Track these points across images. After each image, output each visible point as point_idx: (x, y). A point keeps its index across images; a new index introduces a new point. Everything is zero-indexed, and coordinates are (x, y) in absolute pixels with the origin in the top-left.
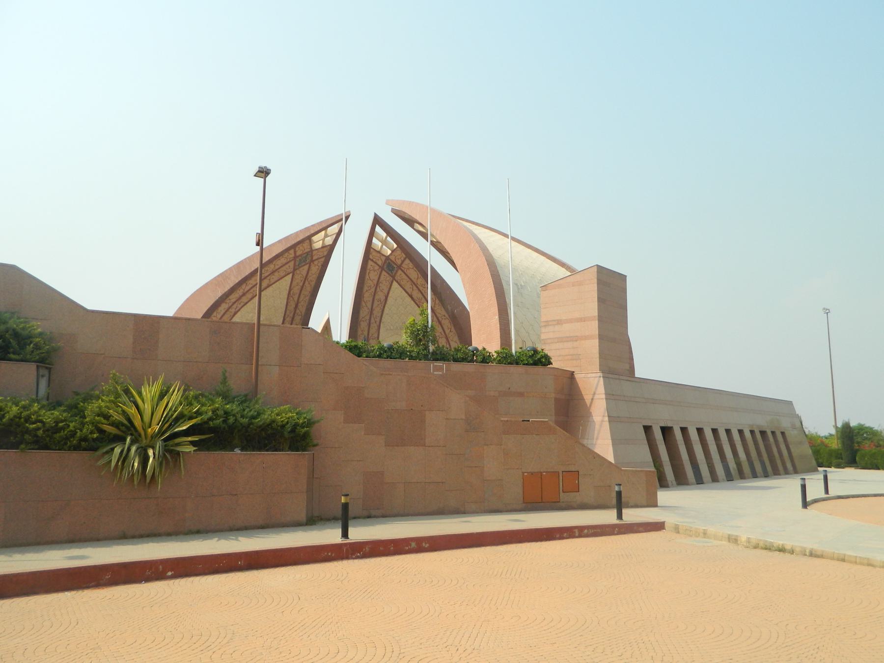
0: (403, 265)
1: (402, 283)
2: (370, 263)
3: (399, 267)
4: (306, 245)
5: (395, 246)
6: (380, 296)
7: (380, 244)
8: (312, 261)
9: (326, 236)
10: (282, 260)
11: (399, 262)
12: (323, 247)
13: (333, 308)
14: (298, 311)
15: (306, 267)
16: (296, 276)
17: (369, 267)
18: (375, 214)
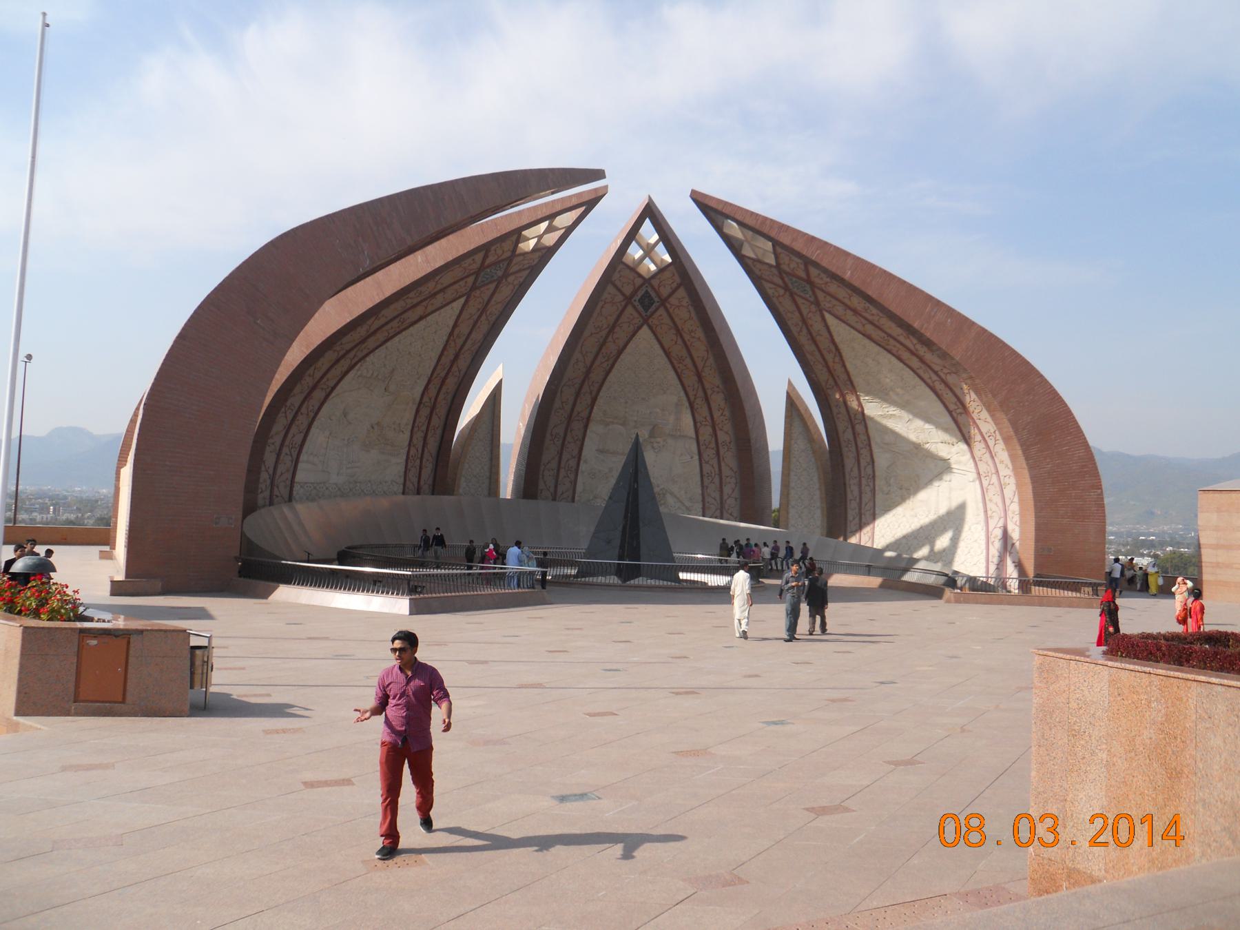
0: (673, 300)
2: (610, 289)
3: (664, 302)
4: (508, 245)
5: (667, 258)
6: (611, 347)
7: (641, 252)
8: (506, 275)
10: (457, 272)
11: (665, 292)
12: (535, 250)
13: (517, 366)
14: (455, 369)
16: (471, 303)
17: (605, 295)
18: (650, 198)
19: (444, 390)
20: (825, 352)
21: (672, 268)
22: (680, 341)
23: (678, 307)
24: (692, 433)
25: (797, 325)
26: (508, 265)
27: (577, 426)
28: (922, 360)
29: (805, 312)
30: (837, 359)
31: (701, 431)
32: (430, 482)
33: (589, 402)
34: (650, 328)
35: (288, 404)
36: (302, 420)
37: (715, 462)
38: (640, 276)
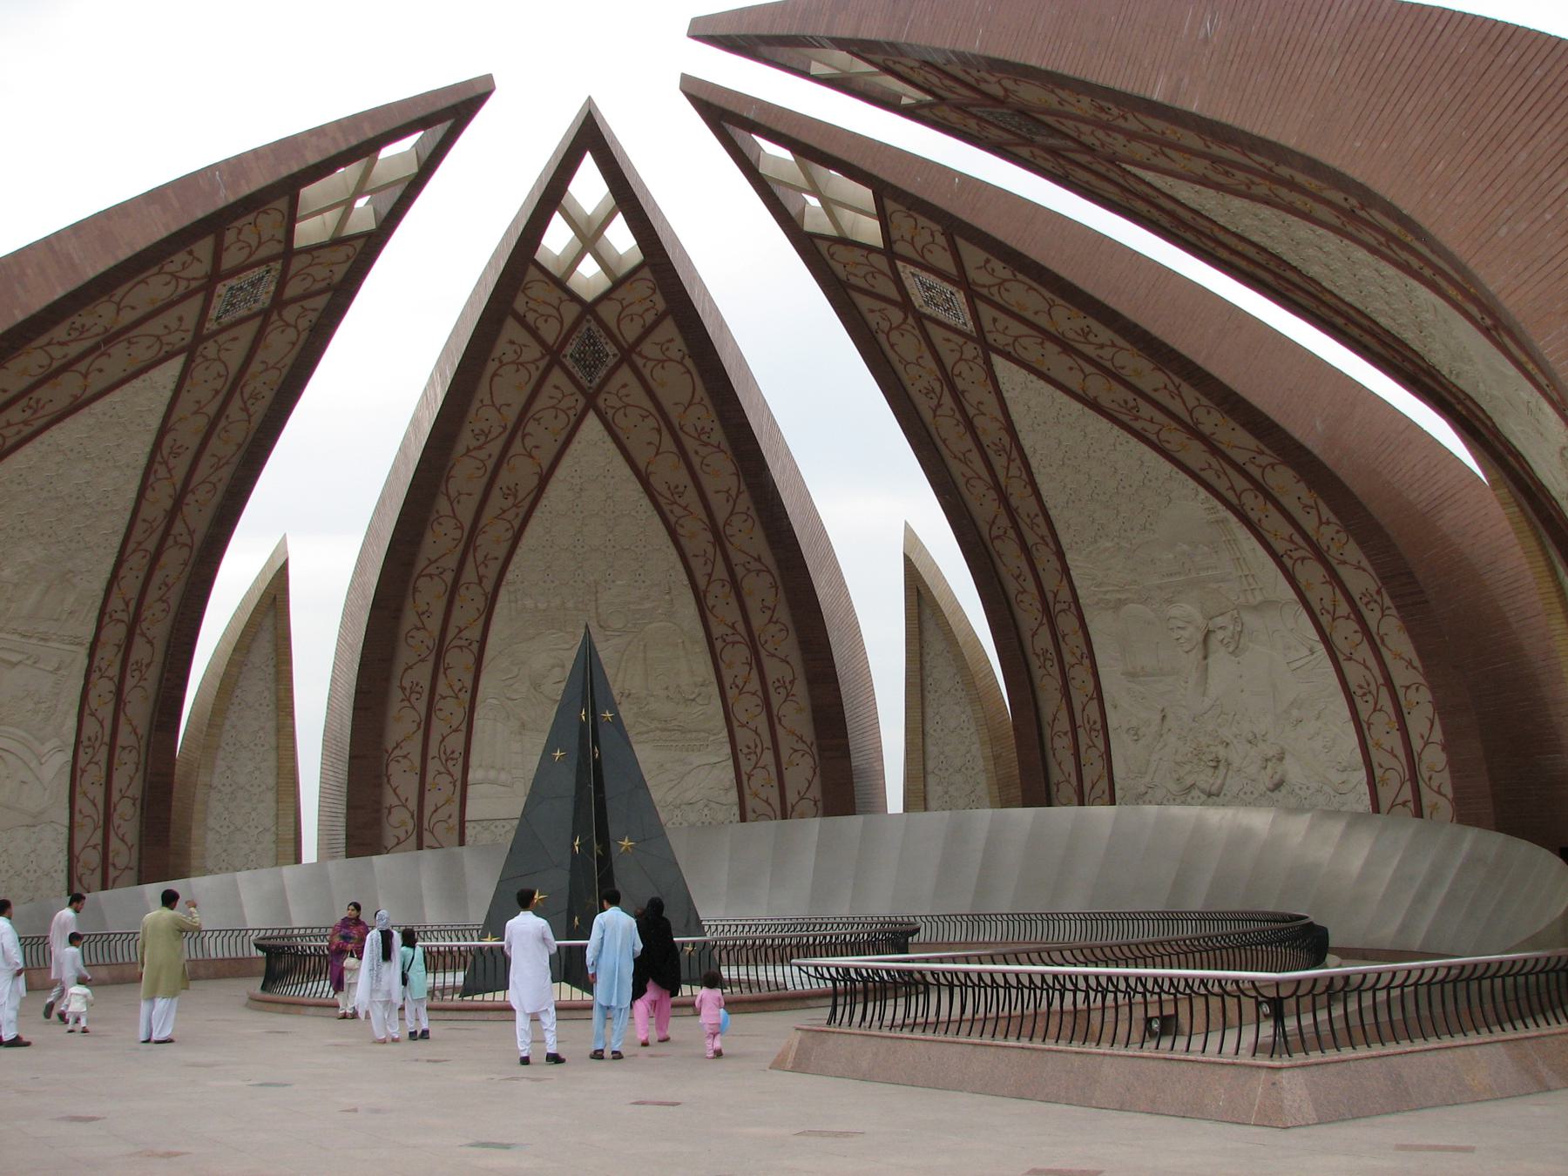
0: (973, 274)
1: (1025, 355)
4: (539, 290)
6: (990, 429)
9: (589, 237)
14: (737, 558)
15: (625, 374)
16: (621, 421)
17: (873, 320)
19: (753, 604)
21: (890, 205)
22: (1088, 369)
23: (1000, 285)
26: (601, 323)
27: (1067, 623)
32: (816, 792)
33: (1054, 563)
34: (1007, 356)
35: (406, 683)
36: (451, 710)
37: (1364, 652)
38: (870, 249)
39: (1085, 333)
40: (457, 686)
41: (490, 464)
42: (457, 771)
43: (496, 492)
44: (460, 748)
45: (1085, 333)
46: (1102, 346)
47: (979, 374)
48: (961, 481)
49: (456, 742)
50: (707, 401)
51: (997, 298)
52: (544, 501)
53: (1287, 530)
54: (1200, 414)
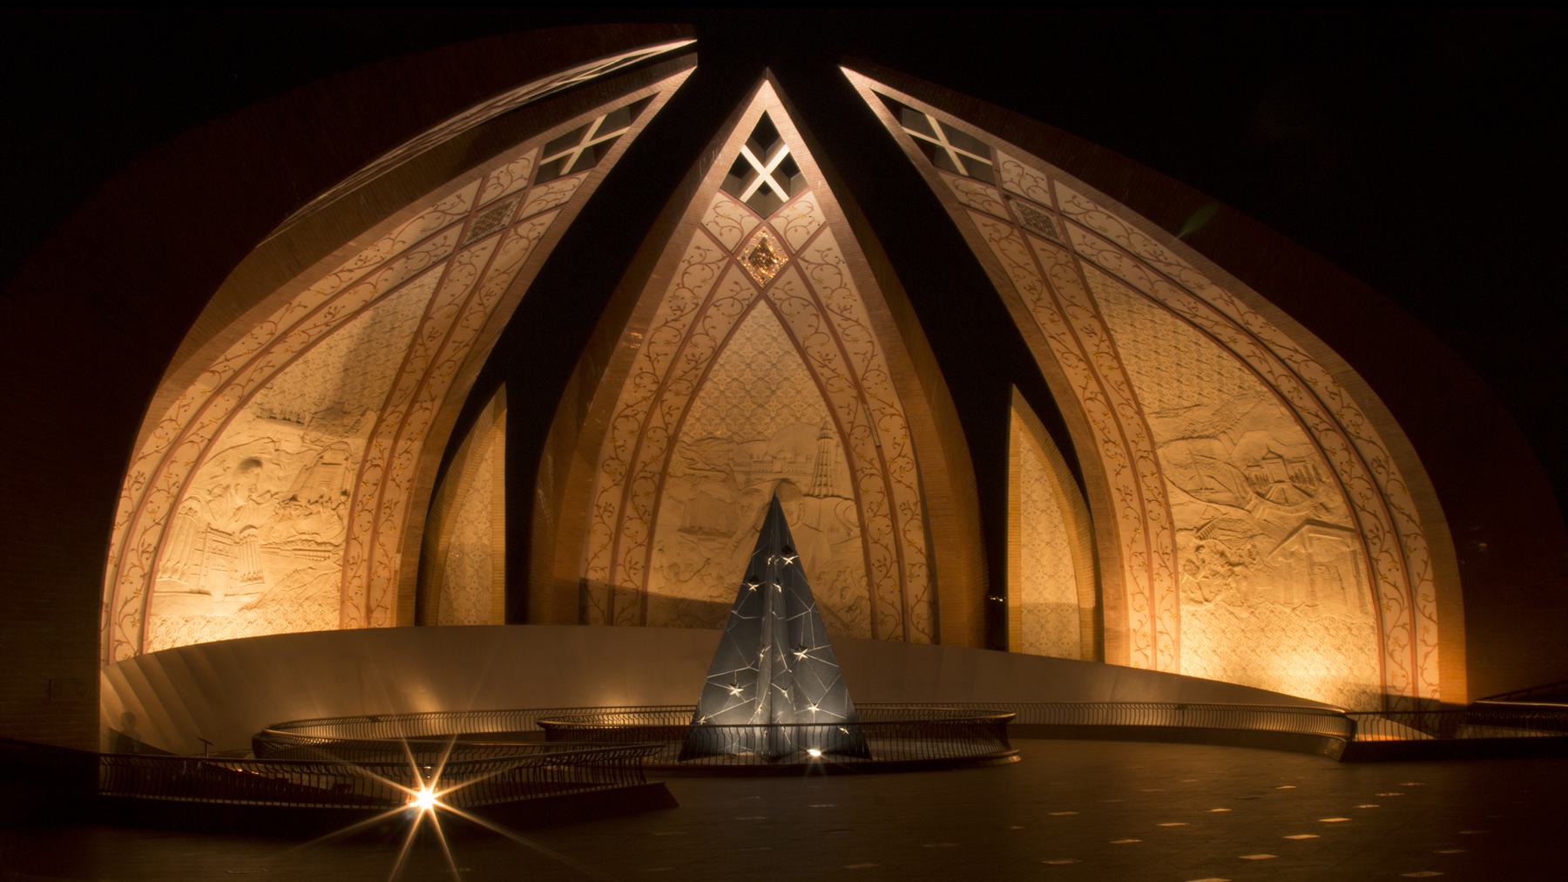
0: (809, 254)
1: (785, 308)
3: (795, 257)
8: (517, 222)
14: (424, 394)
15: (494, 240)
16: (452, 276)
17: (690, 251)
20: (1081, 334)
22: (823, 327)
24: (846, 489)
25: (1032, 289)
26: (521, 204)
28: (1255, 339)
29: (1047, 265)
30: (1104, 346)
31: (865, 483)
34: (772, 305)
37: (889, 540)
39: (845, 309)
40: (174, 479)
41: (344, 285)
42: (147, 564)
43: (326, 310)
44: (154, 544)
45: (845, 309)
46: (847, 319)
47: (737, 309)
48: (635, 370)
49: (152, 538)
50: (513, 275)
51: (808, 273)
52: (349, 326)
53: (872, 453)
54: (872, 376)
